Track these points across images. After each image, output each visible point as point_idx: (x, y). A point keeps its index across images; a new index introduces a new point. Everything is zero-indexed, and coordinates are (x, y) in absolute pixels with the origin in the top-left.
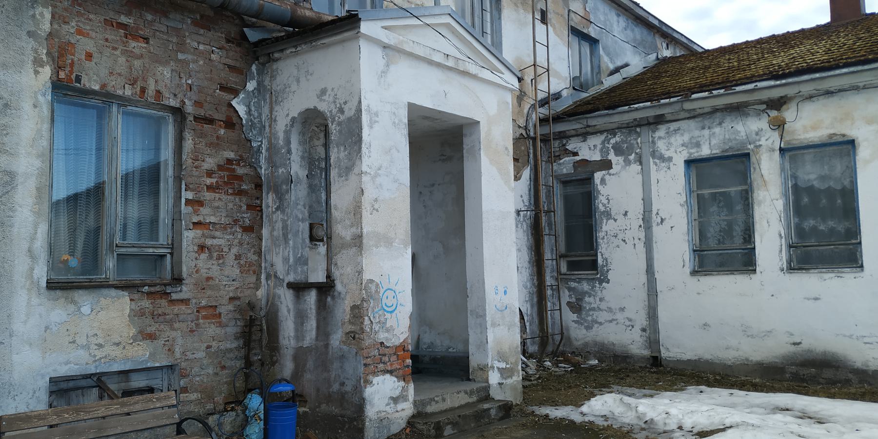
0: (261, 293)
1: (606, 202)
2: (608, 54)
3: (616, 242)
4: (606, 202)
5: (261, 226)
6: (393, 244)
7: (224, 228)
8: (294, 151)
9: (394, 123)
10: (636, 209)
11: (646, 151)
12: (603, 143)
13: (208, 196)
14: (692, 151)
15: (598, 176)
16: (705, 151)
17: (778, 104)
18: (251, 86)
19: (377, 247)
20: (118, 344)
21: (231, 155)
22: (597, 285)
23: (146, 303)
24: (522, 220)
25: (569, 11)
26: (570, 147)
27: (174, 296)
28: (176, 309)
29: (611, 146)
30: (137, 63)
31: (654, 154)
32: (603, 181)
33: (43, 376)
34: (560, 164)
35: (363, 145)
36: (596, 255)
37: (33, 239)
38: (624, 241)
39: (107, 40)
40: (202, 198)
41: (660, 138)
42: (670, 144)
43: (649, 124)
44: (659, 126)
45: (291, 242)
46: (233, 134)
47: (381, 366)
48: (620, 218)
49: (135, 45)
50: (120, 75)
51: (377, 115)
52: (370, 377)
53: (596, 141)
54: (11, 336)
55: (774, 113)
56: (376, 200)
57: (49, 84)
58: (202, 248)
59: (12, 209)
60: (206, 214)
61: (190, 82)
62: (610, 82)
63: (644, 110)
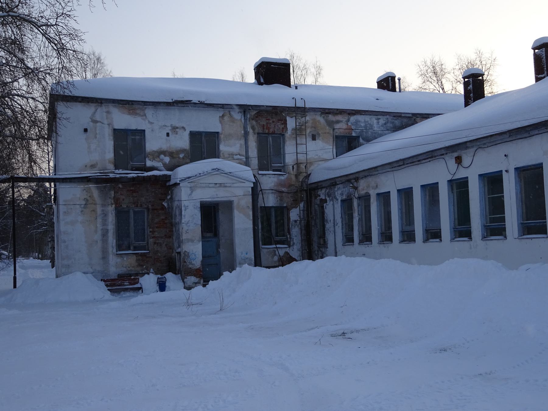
0: (173, 255)
5: (173, 235)
6: (194, 241)
7: (162, 237)
8: (177, 215)
9: (194, 208)
10: (332, 219)
13: (157, 229)
14: (342, 197)
15: (325, 205)
16: (344, 197)
18: (169, 197)
19: (188, 242)
20: (133, 267)
21: (163, 217)
22: (326, 249)
23: (140, 257)
24: (298, 224)
25: (334, 129)
26: (318, 193)
27: (148, 256)
28: (148, 259)
30: (135, 198)
33: (116, 273)
34: (317, 200)
35: (182, 216)
37: (113, 243)
39: (128, 195)
40: (155, 230)
41: (336, 191)
42: (338, 193)
43: (333, 185)
44: (336, 186)
45: (177, 241)
46: (163, 212)
47: (191, 274)
48: (329, 222)
49: (134, 194)
50: (131, 203)
52: (186, 277)
53: (323, 191)
54: (109, 264)
56: (188, 230)
57: (114, 208)
59: (108, 237)
60: (156, 234)
61: (150, 200)
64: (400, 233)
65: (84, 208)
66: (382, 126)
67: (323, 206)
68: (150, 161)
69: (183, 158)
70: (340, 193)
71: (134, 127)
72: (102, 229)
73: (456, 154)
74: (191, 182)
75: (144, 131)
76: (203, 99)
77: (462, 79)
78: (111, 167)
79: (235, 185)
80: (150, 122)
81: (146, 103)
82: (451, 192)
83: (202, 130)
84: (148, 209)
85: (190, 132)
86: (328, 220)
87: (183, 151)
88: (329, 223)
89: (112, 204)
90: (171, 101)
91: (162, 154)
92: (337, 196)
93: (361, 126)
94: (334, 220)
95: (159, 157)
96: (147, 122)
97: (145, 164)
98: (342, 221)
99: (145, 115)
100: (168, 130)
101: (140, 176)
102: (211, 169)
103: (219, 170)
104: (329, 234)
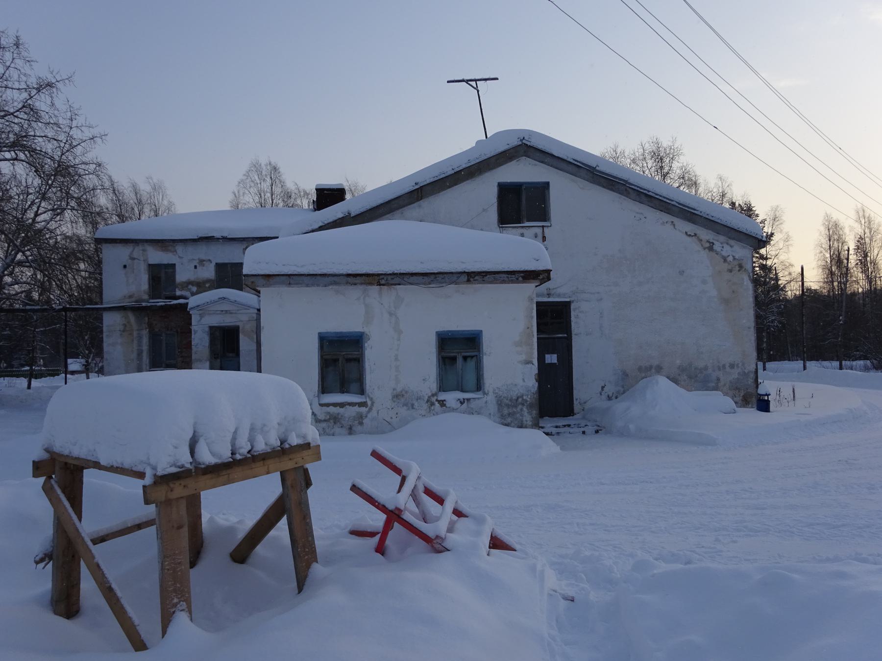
13: (184, 350)
51: (197, 331)
58: (183, 362)
65: (124, 331)
68: (179, 290)
69: (209, 287)
71: (165, 262)
72: (138, 350)
74: (200, 310)
75: (175, 264)
76: (225, 235)
78: (146, 297)
79: (241, 312)
80: (180, 257)
81: (174, 241)
83: (226, 261)
84: (177, 332)
85: (216, 264)
87: (208, 281)
89: (146, 328)
90: (196, 238)
91: (190, 284)
95: (187, 286)
96: (177, 257)
97: (175, 294)
99: (176, 251)
100: (196, 263)
101: (168, 304)
102: (217, 298)
103: (225, 298)
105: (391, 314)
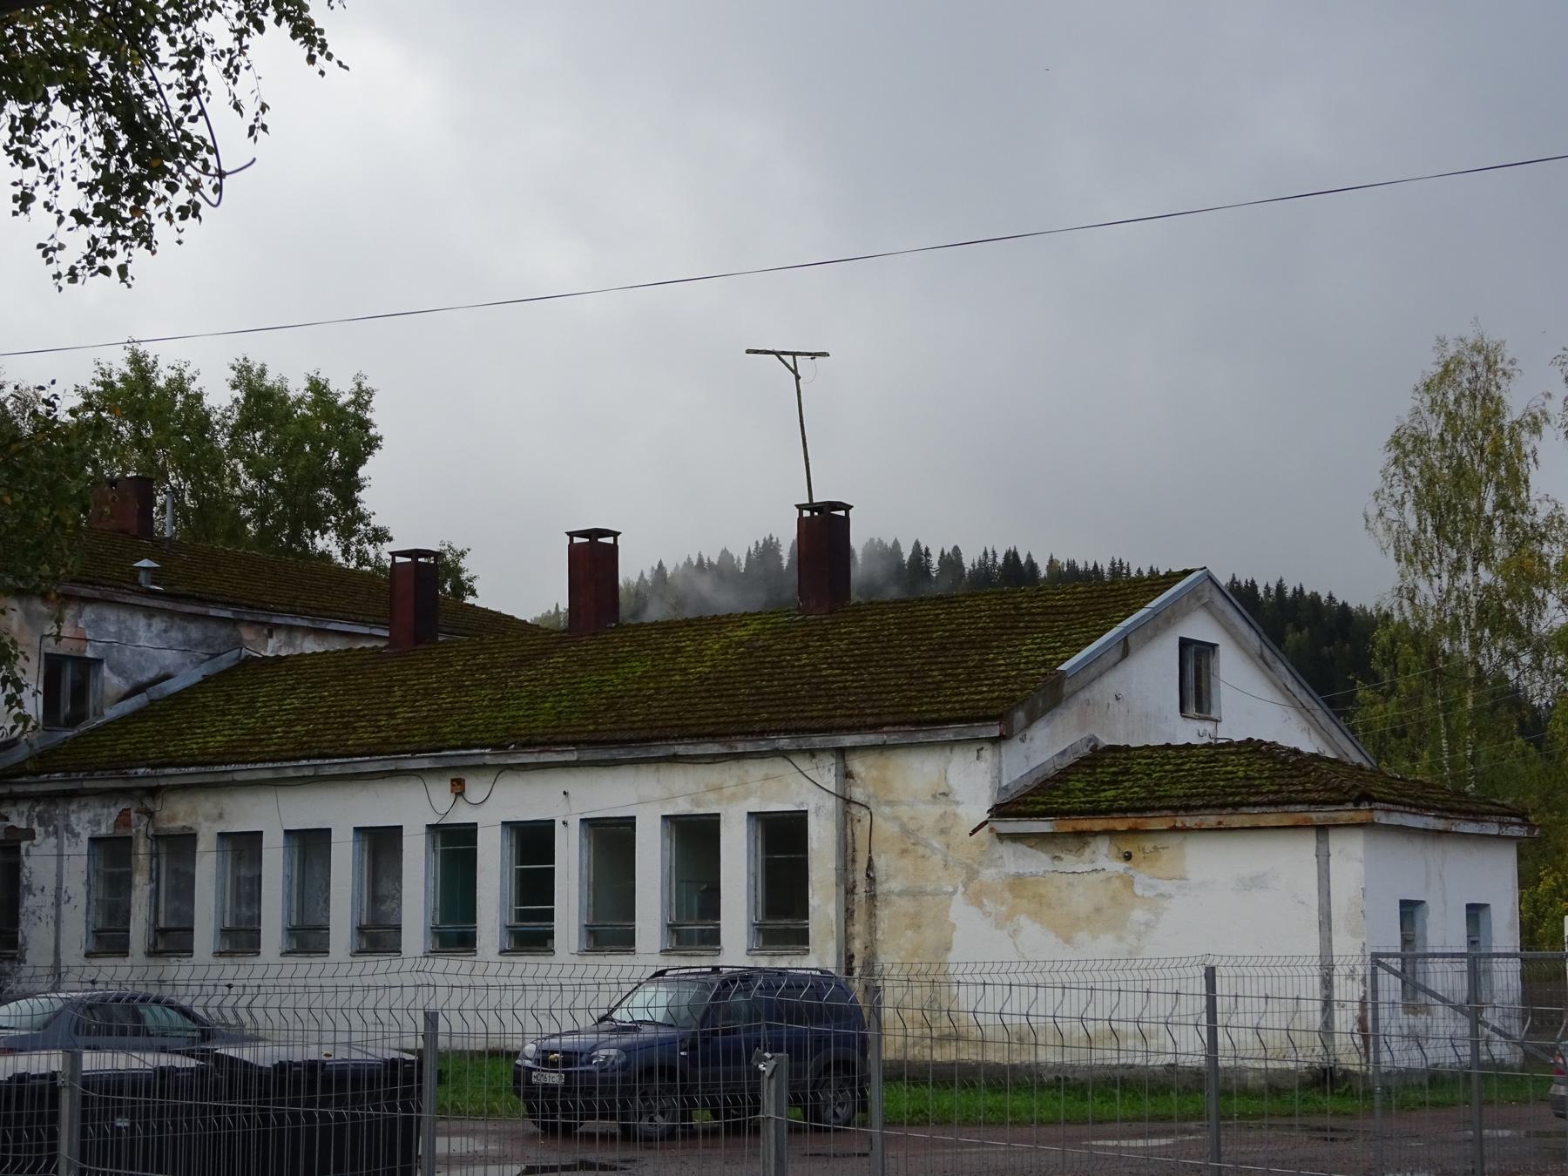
1: (28, 875)
2: (119, 671)
3: (34, 919)
4: (28, 875)
11: (60, 823)
12: (29, 811)
14: (95, 829)
15: (24, 845)
16: (103, 831)
17: (153, 792)
22: (16, 965)
25: (43, 637)
29: (35, 814)
31: (67, 827)
32: (28, 854)
36: (17, 933)
38: (40, 918)
41: (73, 811)
42: (80, 819)
48: (38, 892)
53: (24, 807)
55: (149, 804)
62: (111, 713)
63: (56, 782)
64: (283, 933)
66: (158, 636)
67: (19, 847)
70: (87, 819)
73: (454, 775)
77: (390, 557)
82: (431, 849)
86: (34, 887)
88: (35, 896)
92: (78, 825)
93: (108, 633)
94: (59, 888)
98: (88, 893)
104: (35, 924)
105: (1441, 876)
